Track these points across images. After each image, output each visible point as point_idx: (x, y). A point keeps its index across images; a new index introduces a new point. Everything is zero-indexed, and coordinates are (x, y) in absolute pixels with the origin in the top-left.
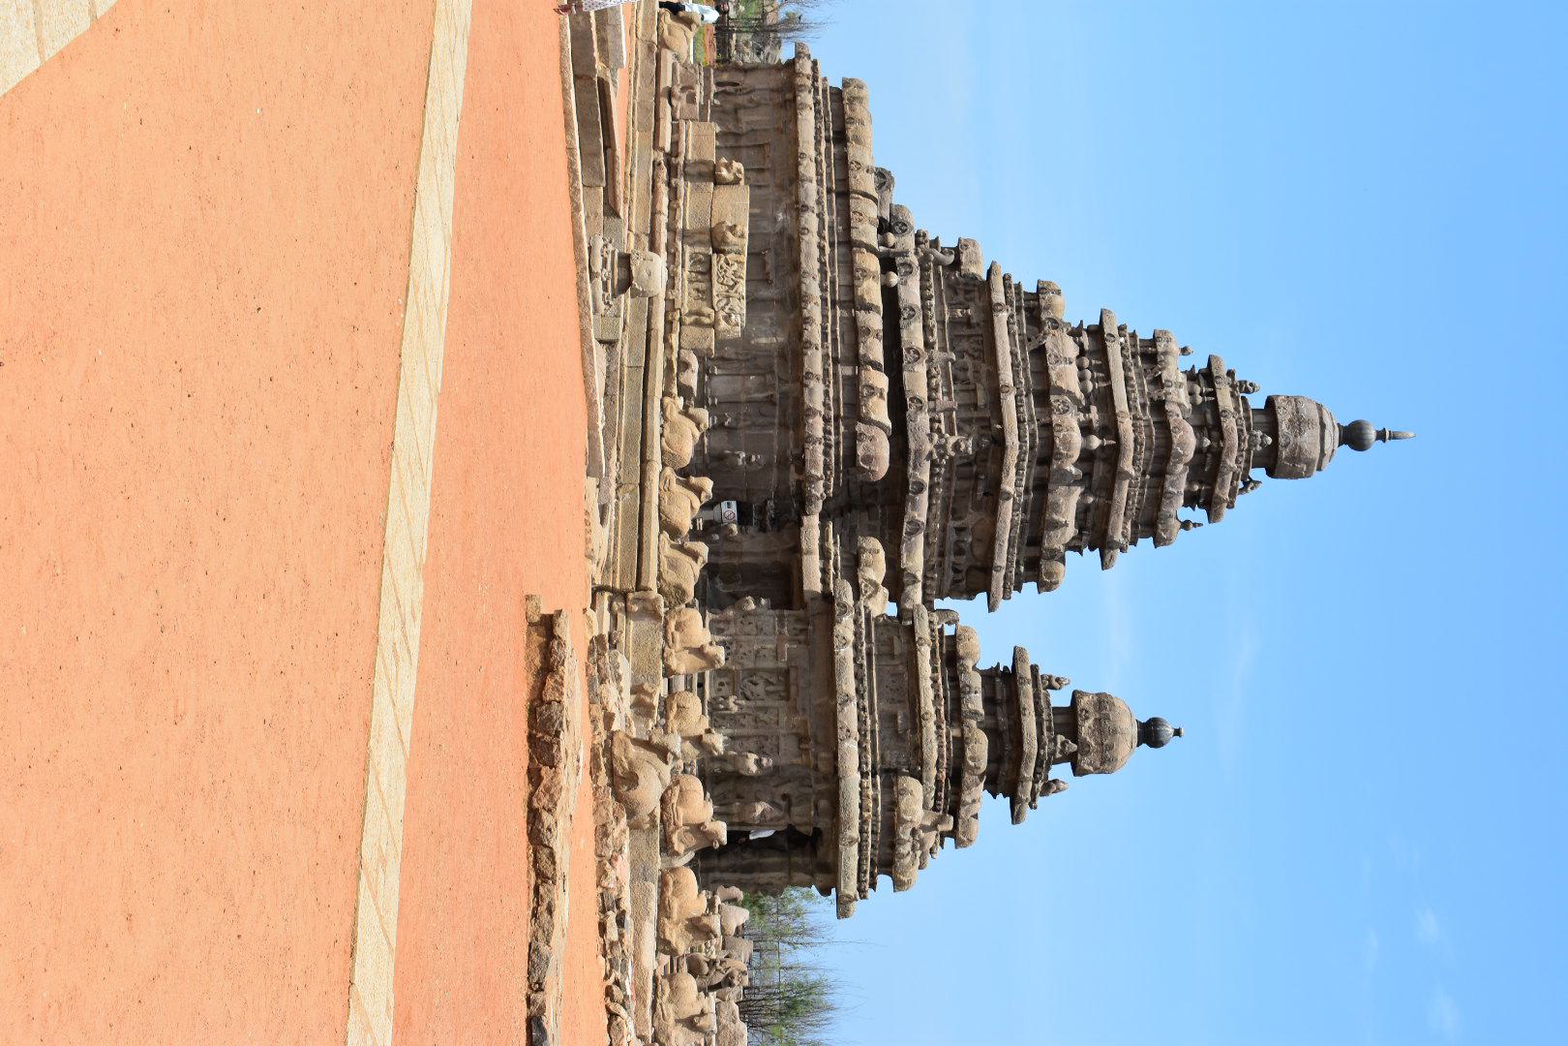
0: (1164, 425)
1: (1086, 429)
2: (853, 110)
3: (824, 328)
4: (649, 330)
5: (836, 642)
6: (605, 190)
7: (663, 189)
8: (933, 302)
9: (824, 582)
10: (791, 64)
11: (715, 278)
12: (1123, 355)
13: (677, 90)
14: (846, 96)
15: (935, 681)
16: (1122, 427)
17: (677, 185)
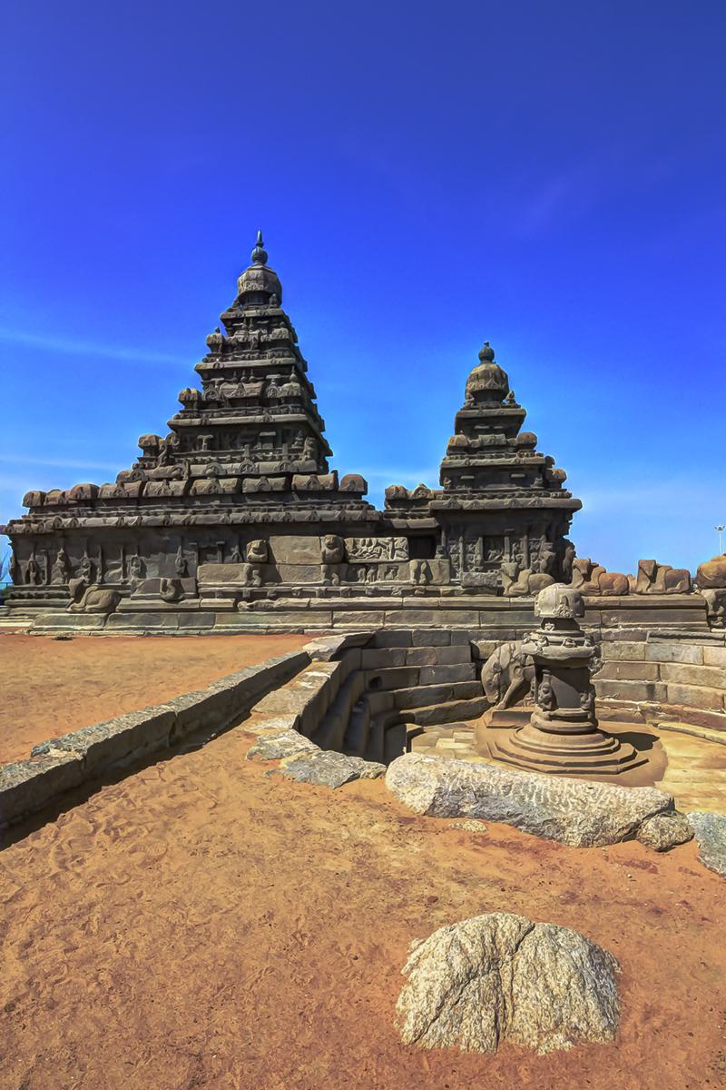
0: (273, 344)
1: (280, 382)
2: (54, 499)
3: (264, 511)
4: (439, 608)
5: (474, 508)
6: (363, 647)
7: (277, 603)
8: (199, 458)
9: (421, 517)
10: (14, 537)
11: (375, 560)
12: (228, 360)
13: (170, 594)
14: (39, 504)
15: (492, 457)
16: (282, 362)
17: (275, 592)
